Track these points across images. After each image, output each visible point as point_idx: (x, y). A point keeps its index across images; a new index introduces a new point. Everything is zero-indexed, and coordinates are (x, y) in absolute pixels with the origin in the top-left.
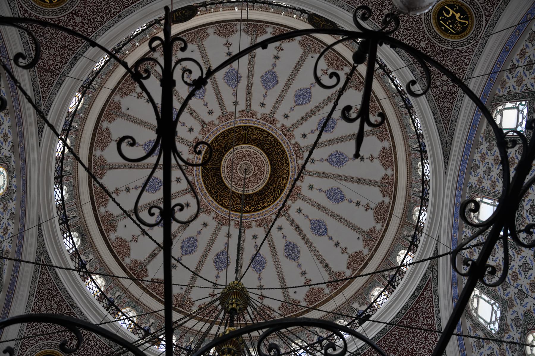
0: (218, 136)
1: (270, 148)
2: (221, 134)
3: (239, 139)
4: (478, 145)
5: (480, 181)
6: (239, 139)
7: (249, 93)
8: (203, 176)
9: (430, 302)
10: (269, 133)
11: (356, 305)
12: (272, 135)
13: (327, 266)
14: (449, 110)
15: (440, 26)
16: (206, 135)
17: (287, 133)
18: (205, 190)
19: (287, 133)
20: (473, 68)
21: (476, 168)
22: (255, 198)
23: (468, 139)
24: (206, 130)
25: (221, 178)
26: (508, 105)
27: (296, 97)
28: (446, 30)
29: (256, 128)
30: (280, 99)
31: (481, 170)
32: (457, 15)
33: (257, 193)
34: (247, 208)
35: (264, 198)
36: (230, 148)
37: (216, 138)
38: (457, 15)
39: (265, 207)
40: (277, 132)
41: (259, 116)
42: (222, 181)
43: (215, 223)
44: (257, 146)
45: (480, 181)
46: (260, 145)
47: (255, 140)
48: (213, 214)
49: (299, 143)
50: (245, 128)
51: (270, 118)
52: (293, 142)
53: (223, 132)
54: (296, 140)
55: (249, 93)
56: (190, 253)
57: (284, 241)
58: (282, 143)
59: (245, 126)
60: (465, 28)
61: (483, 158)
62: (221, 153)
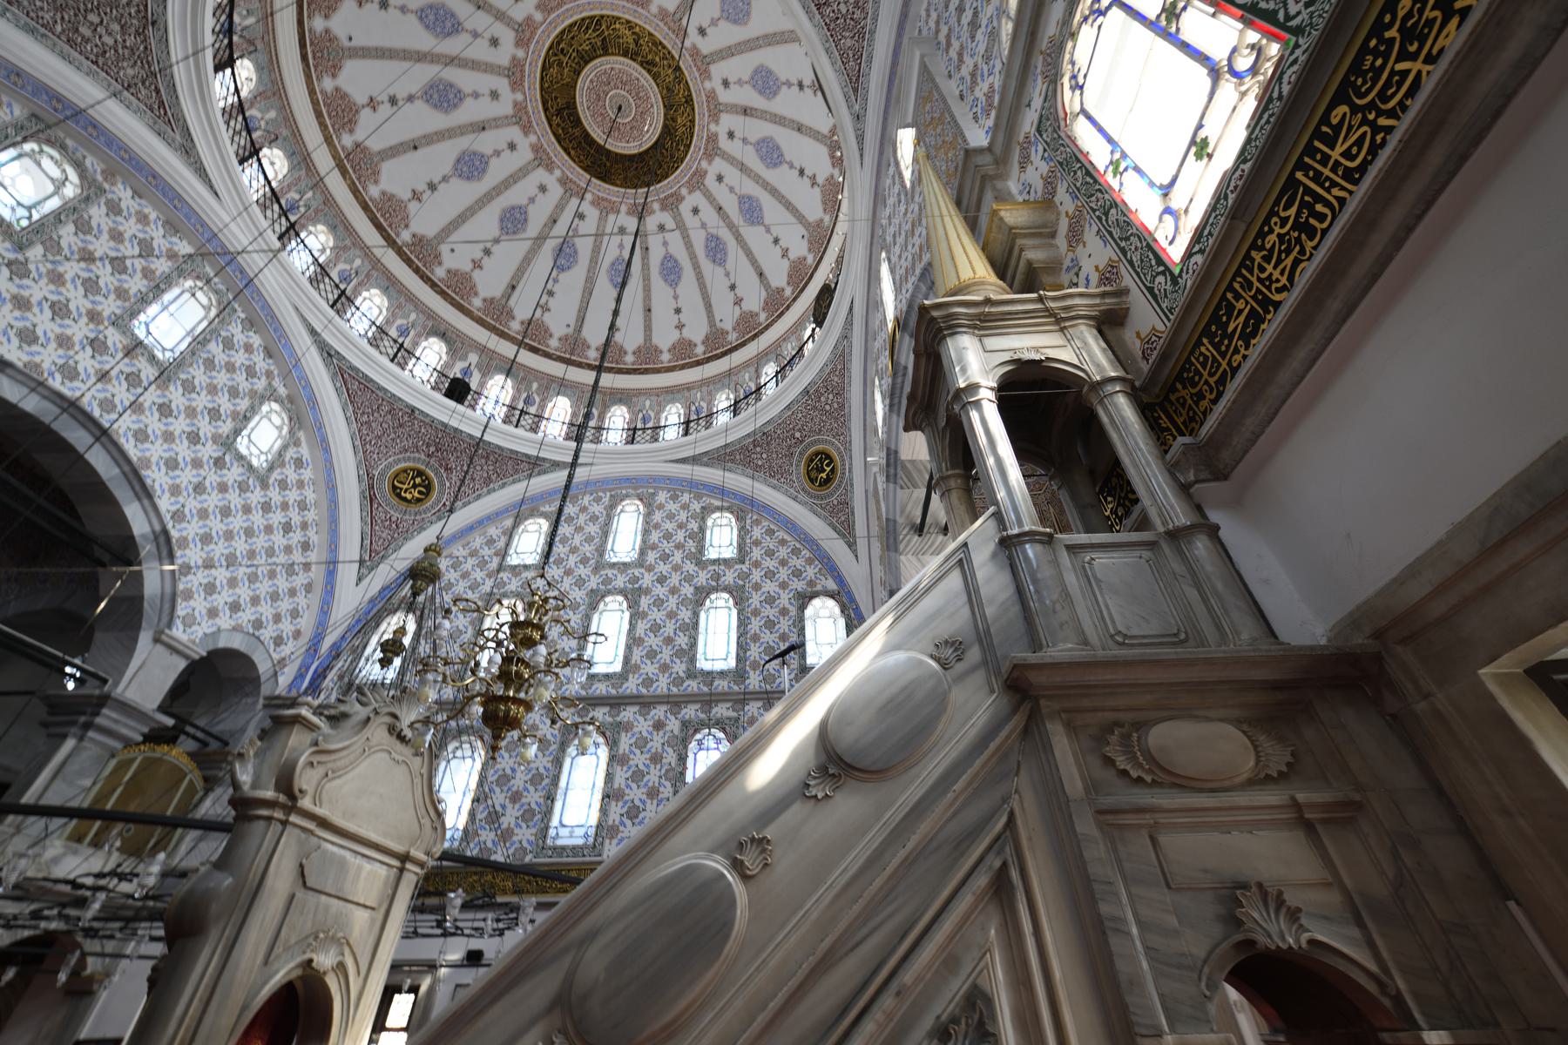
4: (698, 497)
5: (661, 507)
7: (746, 111)
8: (583, 19)
9: (516, 471)
10: (689, 146)
11: (473, 358)
13: (514, 287)
14: (733, 461)
15: (817, 454)
18: (559, 29)
20: (774, 487)
21: (674, 498)
22: (577, 132)
23: (705, 486)
25: (592, 59)
26: (735, 532)
27: (750, 198)
28: (812, 461)
29: (692, 121)
30: (743, 168)
31: (672, 507)
32: (824, 475)
33: (588, 135)
34: (556, 120)
35: (583, 149)
36: (649, 71)
38: (824, 475)
39: (569, 154)
41: (713, 127)
42: (587, 63)
43: (505, 61)
44: (665, 126)
45: (661, 507)
46: (668, 130)
47: (674, 120)
48: (520, 54)
50: (689, 100)
51: (713, 151)
52: (684, 191)
54: (688, 198)
55: (746, 111)
56: (427, 27)
57: (525, 202)
60: (812, 481)
61: (685, 507)
62: (637, 54)
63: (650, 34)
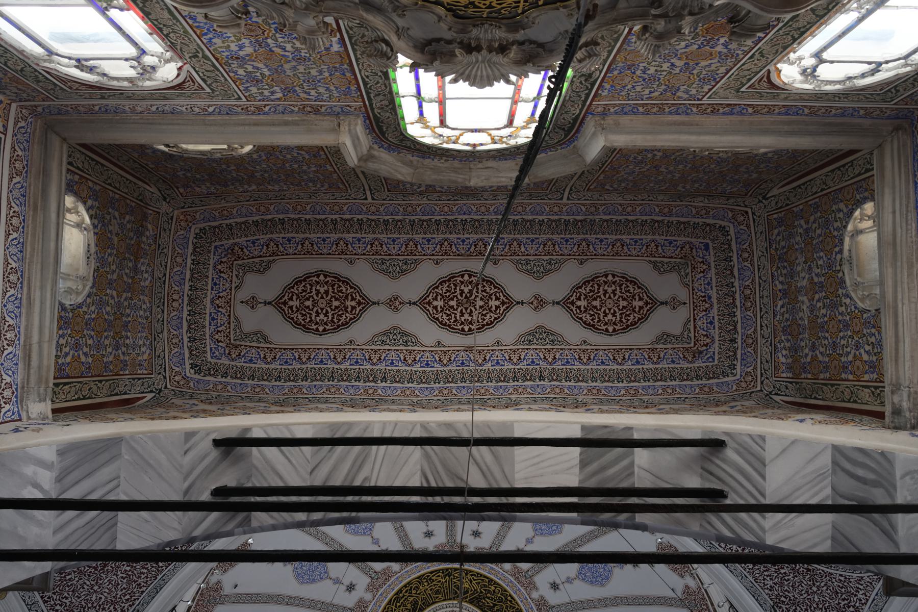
0: (400, 591)
1: (495, 605)
2: (405, 586)
3: (438, 592)
6: (438, 592)
10: (491, 580)
12: (495, 583)
16: (378, 591)
17: (523, 580)
19: (523, 580)
24: (377, 584)
37: (397, 594)
40: (506, 578)
49: (547, 597)
53: (409, 583)
58: (515, 596)
59: (447, 569)
63: (389, 603)
